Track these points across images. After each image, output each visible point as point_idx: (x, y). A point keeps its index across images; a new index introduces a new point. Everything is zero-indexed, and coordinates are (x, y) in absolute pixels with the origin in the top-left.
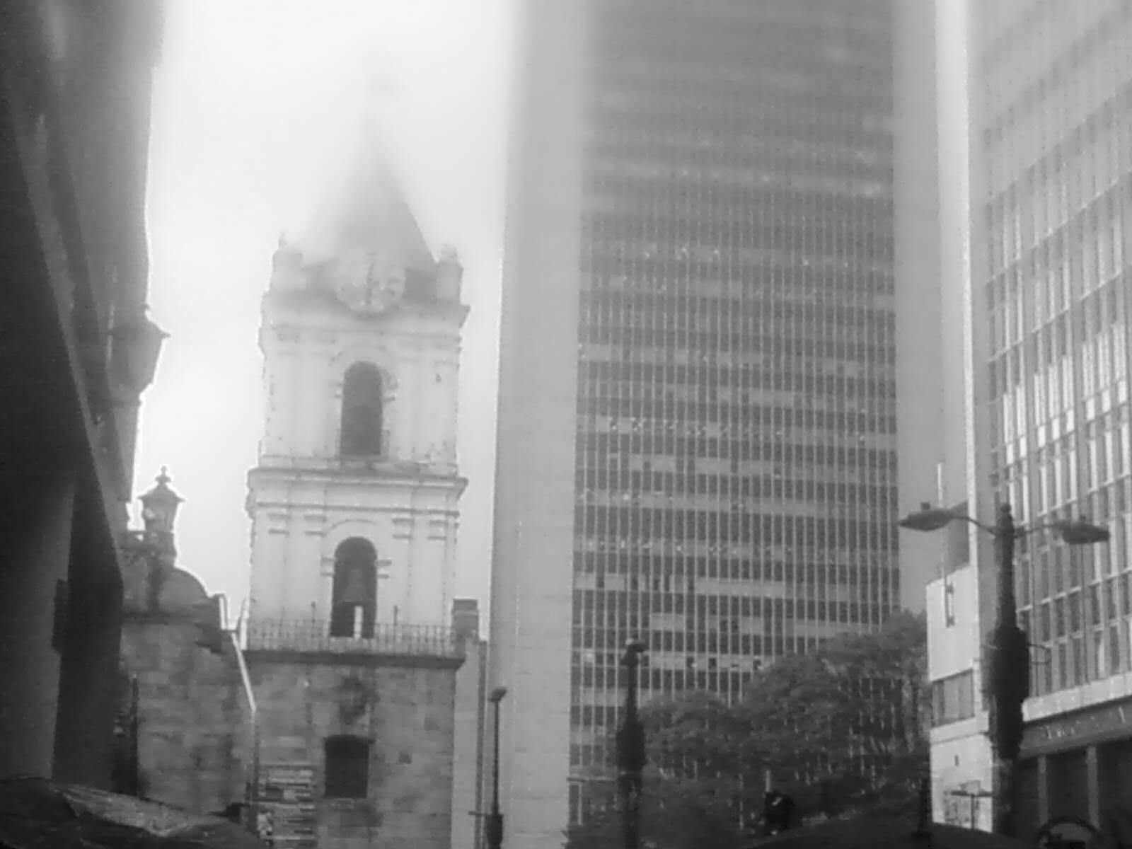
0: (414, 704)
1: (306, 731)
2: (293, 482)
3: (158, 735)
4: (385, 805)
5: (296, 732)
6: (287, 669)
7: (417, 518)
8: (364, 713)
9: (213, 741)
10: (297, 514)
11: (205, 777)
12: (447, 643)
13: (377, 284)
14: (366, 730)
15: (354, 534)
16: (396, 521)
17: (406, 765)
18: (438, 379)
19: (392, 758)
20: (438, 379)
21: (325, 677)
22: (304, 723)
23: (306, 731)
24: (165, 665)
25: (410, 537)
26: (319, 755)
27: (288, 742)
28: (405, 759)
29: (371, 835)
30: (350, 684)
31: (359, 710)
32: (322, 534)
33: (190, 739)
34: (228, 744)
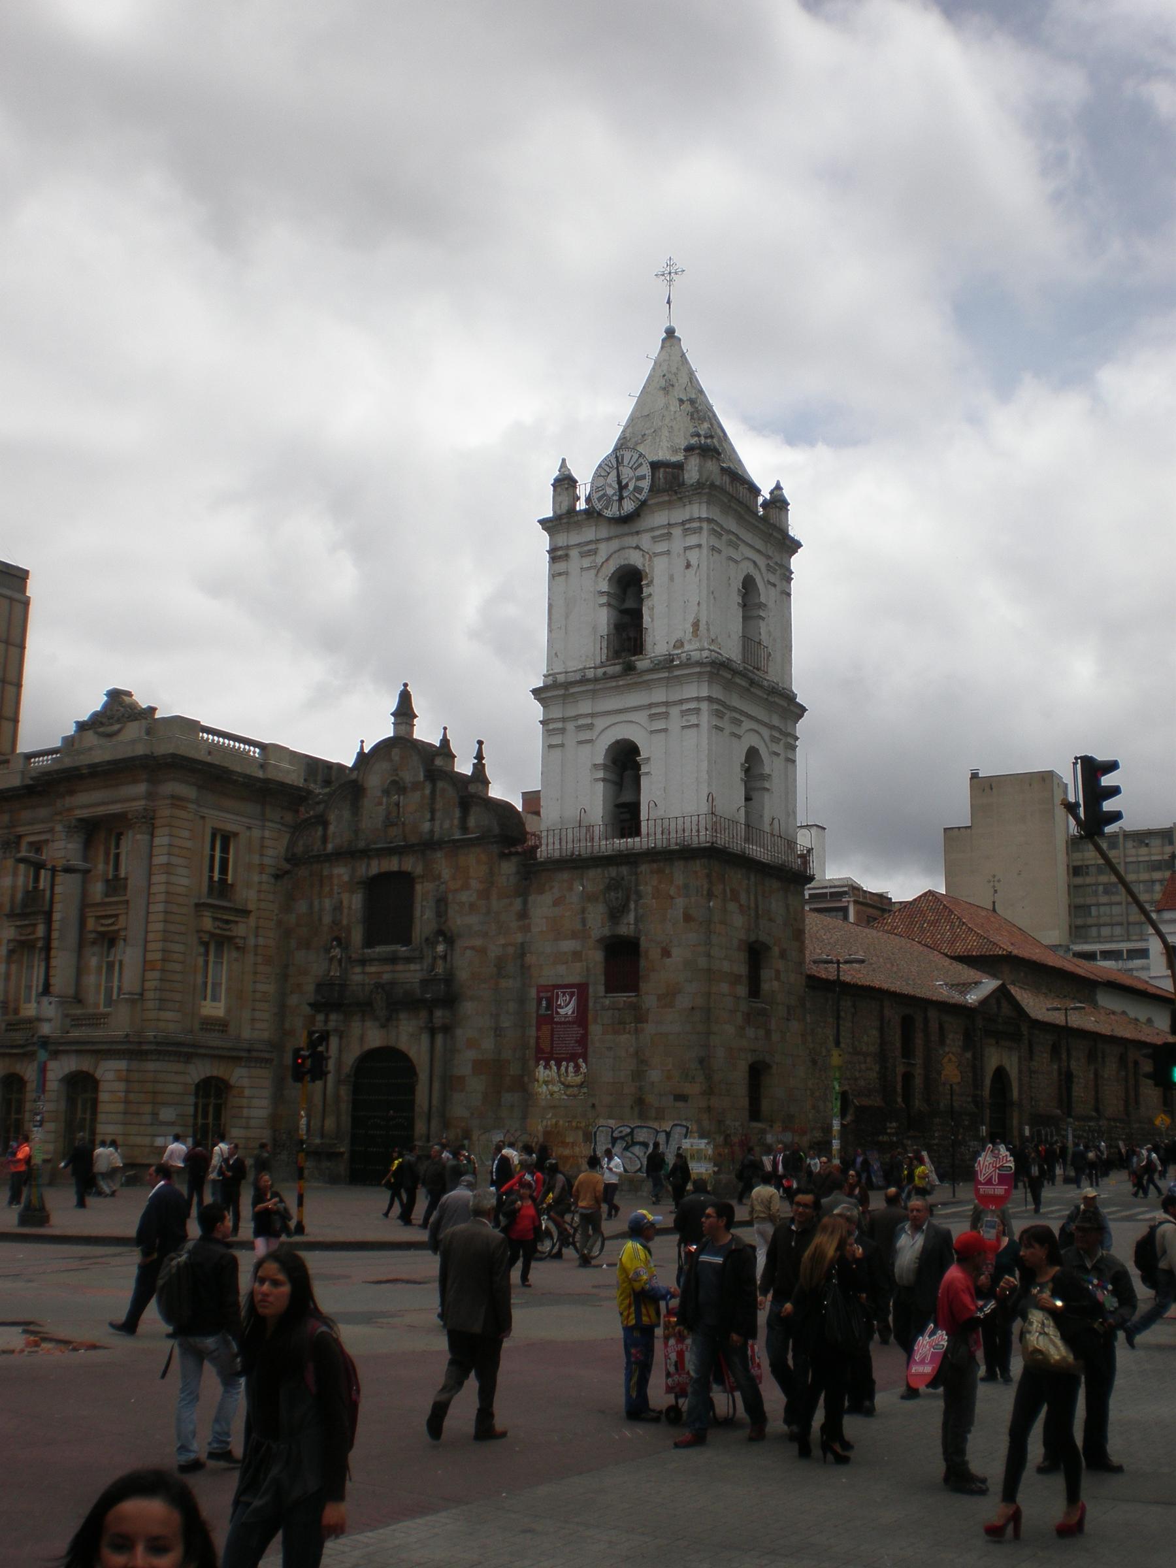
0: (672, 898)
2: (564, 695)
3: (467, 948)
4: (650, 1001)
5: (574, 935)
6: (566, 875)
8: (629, 911)
9: (511, 950)
10: (570, 726)
11: (504, 983)
13: (627, 485)
14: (632, 927)
16: (653, 717)
17: (668, 961)
18: (688, 566)
19: (654, 953)
20: (688, 566)
21: (594, 880)
22: (579, 927)
24: (474, 884)
26: (597, 957)
27: (568, 945)
28: (666, 953)
29: (637, 1031)
30: (614, 885)
31: (623, 909)
33: (494, 952)
34: (522, 951)
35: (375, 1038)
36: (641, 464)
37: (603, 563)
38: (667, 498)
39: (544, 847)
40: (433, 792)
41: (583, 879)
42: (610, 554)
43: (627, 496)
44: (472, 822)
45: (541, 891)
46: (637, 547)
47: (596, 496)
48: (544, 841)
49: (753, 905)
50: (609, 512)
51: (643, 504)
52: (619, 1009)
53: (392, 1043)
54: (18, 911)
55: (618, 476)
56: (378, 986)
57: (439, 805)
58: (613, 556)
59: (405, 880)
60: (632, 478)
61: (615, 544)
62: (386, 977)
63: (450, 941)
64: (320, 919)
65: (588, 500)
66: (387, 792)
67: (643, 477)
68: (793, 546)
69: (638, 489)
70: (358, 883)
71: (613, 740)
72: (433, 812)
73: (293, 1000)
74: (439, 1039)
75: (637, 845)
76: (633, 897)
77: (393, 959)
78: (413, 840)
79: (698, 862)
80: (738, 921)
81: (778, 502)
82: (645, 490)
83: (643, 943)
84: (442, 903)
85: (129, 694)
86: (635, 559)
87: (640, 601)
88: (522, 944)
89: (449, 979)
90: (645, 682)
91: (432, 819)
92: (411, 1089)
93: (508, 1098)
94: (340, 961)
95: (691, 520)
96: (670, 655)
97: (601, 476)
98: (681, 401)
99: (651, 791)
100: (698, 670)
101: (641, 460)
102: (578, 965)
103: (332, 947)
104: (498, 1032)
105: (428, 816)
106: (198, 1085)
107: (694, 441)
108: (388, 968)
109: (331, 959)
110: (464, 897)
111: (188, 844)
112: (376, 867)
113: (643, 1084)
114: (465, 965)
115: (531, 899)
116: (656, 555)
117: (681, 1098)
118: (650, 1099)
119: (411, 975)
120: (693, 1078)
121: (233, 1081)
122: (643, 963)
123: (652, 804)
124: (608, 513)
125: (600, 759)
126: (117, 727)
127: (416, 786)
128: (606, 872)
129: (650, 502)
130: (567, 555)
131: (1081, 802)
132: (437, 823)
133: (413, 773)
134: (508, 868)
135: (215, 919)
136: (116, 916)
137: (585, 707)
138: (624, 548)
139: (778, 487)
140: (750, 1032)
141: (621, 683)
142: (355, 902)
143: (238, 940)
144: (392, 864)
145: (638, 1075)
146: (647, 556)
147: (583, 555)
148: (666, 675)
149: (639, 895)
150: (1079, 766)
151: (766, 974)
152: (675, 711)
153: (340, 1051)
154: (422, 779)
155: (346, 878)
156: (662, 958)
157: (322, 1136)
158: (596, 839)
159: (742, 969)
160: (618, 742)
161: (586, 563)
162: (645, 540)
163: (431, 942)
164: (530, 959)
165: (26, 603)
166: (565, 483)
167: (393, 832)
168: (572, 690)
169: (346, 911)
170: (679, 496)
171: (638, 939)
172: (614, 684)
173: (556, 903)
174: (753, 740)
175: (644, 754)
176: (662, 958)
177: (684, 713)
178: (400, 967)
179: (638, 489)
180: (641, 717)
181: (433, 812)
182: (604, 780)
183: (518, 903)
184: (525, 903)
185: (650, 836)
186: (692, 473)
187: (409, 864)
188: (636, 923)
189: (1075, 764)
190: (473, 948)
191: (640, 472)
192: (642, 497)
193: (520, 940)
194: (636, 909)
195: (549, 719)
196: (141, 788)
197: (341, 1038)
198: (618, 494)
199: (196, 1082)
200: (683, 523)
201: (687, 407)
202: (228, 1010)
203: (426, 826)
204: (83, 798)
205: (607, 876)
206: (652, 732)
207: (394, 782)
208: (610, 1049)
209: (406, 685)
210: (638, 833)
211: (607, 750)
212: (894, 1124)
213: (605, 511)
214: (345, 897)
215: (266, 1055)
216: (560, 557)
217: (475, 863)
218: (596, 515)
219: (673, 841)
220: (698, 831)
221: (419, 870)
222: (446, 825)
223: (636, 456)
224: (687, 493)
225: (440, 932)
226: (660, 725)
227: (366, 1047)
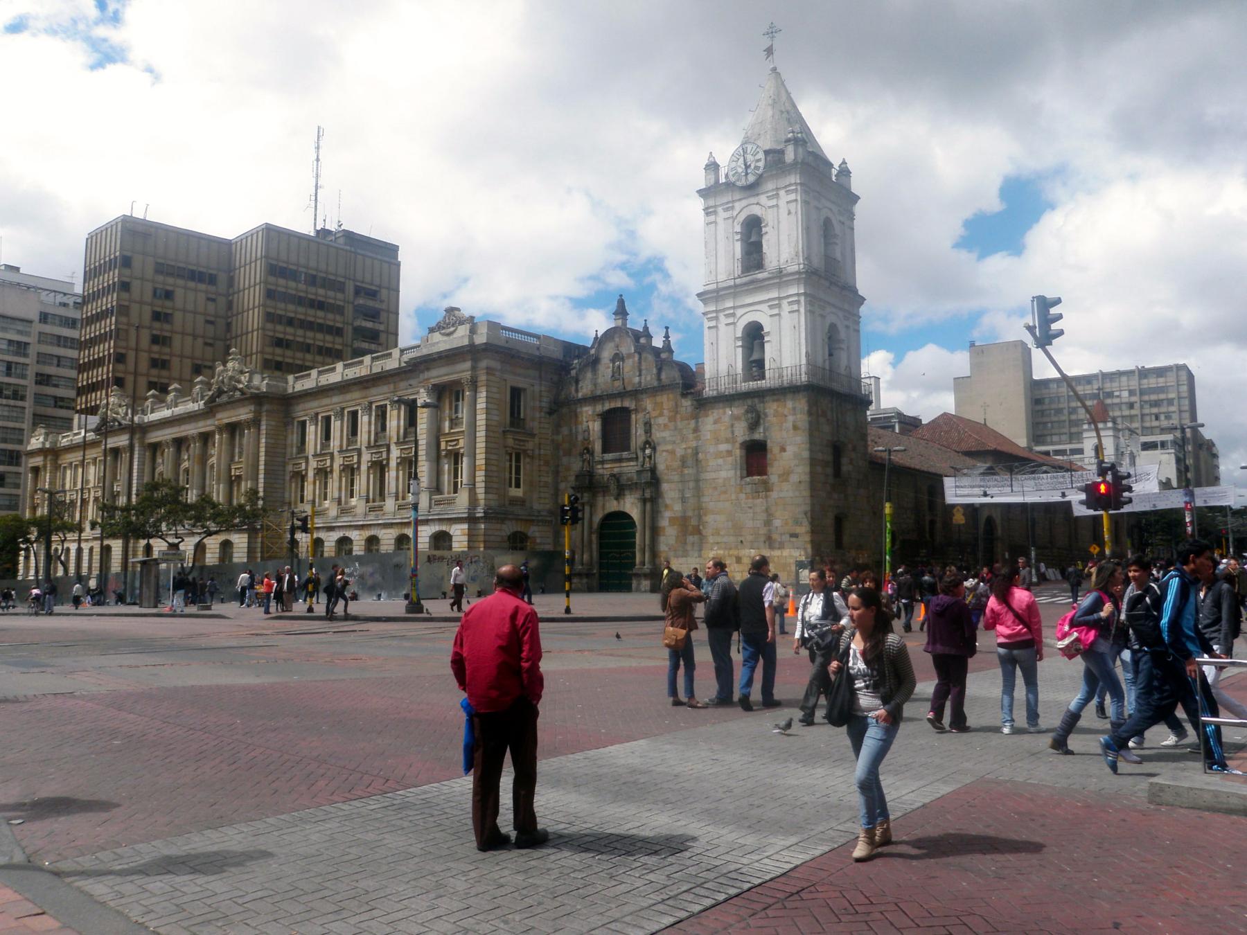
0: (786, 416)
1: (731, 440)
3: (663, 451)
4: (773, 478)
5: (727, 441)
9: (690, 451)
11: (686, 471)
12: (803, 376)
16: (771, 307)
18: (789, 213)
19: (776, 450)
21: (738, 410)
22: (730, 436)
23: (731, 440)
24: (666, 412)
25: (779, 315)
27: (724, 447)
28: (783, 449)
29: (766, 497)
32: (734, 324)
33: (680, 452)
34: (696, 452)
35: (612, 506)
39: (707, 389)
40: (640, 359)
44: (663, 376)
46: (758, 204)
47: (731, 174)
48: (707, 385)
49: (835, 419)
51: (761, 176)
53: (622, 509)
54: (401, 440)
55: (745, 160)
56: (613, 475)
57: (643, 367)
59: (626, 412)
61: (744, 203)
62: (616, 471)
63: (654, 449)
64: (577, 438)
65: (727, 176)
66: (613, 360)
67: (759, 160)
68: (855, 199)
69: (757, 168)
70: (598, 415)
72: (640, 371)
73: (562, 486)
74: (648, 506)
75: (764, 385)
77: (620, 460)
78: (629, 388)
80: (826, 428)
81: (845, 172)
83: (769, 444)
84: (648, 426)
85: (458, 309)
86: (757, 211)
87: (761, 236)
88: (697, 447)
89: (653, 470)
91: (640, 375)
92: (634, 537)
93: (690, 539)
94: (589, 462)
95: (790, 185)
98: (782, 112)
99: (769, 352)
100: (797, 276)
101: (758, 150)
102: (730, 459)
103: (584, 453)
105: (638, 374)
106: (509, 537)
107: (790, 135)
108: (618, 465)
109: (584, 461)
110: (661, 421)
111: (497, 396)
112: (607, 406)
114: (663, 462)
115: (700, 420)
117: (794, 535)
118: (775, 536)
119: (630, 469)
121: (529, 534)
122: (769, 456)
123: (772, 360)
124: (739, 184)
125: (739, 334)
126: (452, 329)
127: (629, 356)
131: (1037, 325)
132: (643, 377)
133: (628, 347)
134: (687, 403)
135: (515, 439)
136: (458, 440)
137: (729, 304)
139: (844, 162)
140: (835, 496)
142: (596, 427)
143: (529, 452)
144: (617, 404)
145: (768, 523)
147: (726, 210)
148: (778, 281)
149: (766, 415)
150: (1035, 302)
151: (845, 461)
152: (785, 303)
153: (591, 515)
154: (633, 351)
155: (590, 413)
157: (582, 564)
158: (739, 382)
159: (830, 458)
160: (750, 323)
162: (763, 199)
163: (644, 449)
164: (701, 456)
165: (398, 265)
166: (713, 167)
167: (617, 384)
169: (591, 432)
171: (765, 442)
172: (746, 288)
173: (715, 422)
174: (831, 319)
175: (766, 330)
177: (790, 303)
178: (624, 464)
179: (757, 168)
180: (764, 307)
181: (640, 371)
182: (742, 346)
183: (692, 424)
185: (770, 381)
186: (790, 156)
187: (629, 403)
188: (764, 433)
189: (1033, 301)
190: (667, 451)
191: (758, 157)
192: (759, 172)
196: (468, 365)
197: (591, 507)
199: (509, 534)
200: (786, 187)
201: (785, 115)
202: (525, 493)
203: (637, 380)
204: (434, 373)
206: (771, 316)
207: (616, 354)
208: (750, 508)
209: (621, 296)
210: (763, 377)
211: (744, 329)
212: (924, 551)
214: (590, 424)
215: (549, 519)
216: (711, 212)
217: (666, 400)
219: (785, 382)
220: (800, 375)
221: (633, 407)
222: (649, 378)
223: (755, 147)
225: (647, 442)
226: (775, 311)
227: (607, 511)
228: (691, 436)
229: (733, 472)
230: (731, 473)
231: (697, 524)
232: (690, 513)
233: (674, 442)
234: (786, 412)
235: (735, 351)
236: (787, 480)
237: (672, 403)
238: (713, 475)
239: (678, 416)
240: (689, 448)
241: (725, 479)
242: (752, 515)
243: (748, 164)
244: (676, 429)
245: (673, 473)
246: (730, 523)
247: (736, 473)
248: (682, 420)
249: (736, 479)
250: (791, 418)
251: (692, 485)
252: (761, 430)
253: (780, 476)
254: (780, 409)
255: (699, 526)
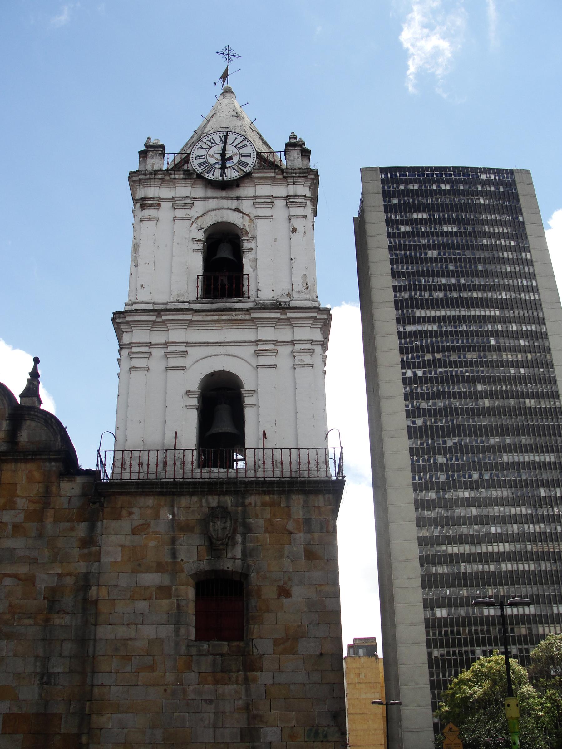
0: (291, 533)
5: (160, 567)
6: (150, 501)
7: (280, 349)
8: (234, 544)
9: (70, 581)
11: (57, 620)
13: (230, 158)
14: (239, 562)
15: (218, 368)
17: (287, 601)
20: (294, 230)
22: (168, 559)
24: (21, 503)
28: (284, 592)
29: (246, 680)
31: (229, 542)
36: (246, 146)
37: (198, 217)
38: (273, 175)
41: (173, 506)
42: (207, 210)
43: (230, 167)
44: (24, 437)
45: (117, 517)
46: (237, 210)
50: (210, 175)
51: (248, 175)
52: (222, 655)
55: (224, 149)
58: (210, 213)
60: (236, 154)
61: (212, 204)
71: (210, 371)
76: (240, 529)
79: (321, 498)
82: (250, 165)
88: (86, 576)
90: (253, 320)
96: (278, 301)
97: (202, 148)
100: (314, 315)
101: (245, 142)
102: (165, 602)
104: (45, 679)
113: (256, 744)
116: (257, 217)
120: (326, 736)
122: (253, 602)
124: (210, 176)
128: (204, 500)
129: (254, 175)
130: (159, 205)
138: (222, 209)
141: (224, 318)
146: (247, 218)
149: (248, 529)
156: (278, 598)
161: (180, 213)
168: (165, 317)
170: (285, 174)
172: (216, 318)
173: (134, 531)
176: (278, 598)
183: (81, 529)
184: (92, 528)
190: (15, 576)
192: (247, 169)
193: (84, 571)
194: (243, 542)
195: (132, 343)
198: (221, 163)
205: (204, 504)
208: (210, 702)
213: (207, 175)
218: (195, 176)
223: (240, 139)
224: (294, 175)
228: (76, 552)
229: (171, 628)
230: (166, 631)
231: (74, 730)
232: (59, 708)
233: (34, 561)
234: (290, 526)
235: (257, 385)
236: (292, 651)
237: (36, 489)
238: (122, 632)
239: (50, 513)
240: (70, 575)
241: (151, 642)
242: (212, 716)
243: (227, 156)
244: (40, 536)
245: (27, 621)
246: (159, 734)
247: (177, 631)
248: (56, 521)
249: (177, 644)
250: (300, 537)
251: (68, 648)
252: (238, 551)
253: (276, 642)
254: (277, 520)
255: (79, 736)
